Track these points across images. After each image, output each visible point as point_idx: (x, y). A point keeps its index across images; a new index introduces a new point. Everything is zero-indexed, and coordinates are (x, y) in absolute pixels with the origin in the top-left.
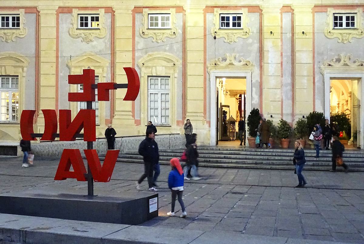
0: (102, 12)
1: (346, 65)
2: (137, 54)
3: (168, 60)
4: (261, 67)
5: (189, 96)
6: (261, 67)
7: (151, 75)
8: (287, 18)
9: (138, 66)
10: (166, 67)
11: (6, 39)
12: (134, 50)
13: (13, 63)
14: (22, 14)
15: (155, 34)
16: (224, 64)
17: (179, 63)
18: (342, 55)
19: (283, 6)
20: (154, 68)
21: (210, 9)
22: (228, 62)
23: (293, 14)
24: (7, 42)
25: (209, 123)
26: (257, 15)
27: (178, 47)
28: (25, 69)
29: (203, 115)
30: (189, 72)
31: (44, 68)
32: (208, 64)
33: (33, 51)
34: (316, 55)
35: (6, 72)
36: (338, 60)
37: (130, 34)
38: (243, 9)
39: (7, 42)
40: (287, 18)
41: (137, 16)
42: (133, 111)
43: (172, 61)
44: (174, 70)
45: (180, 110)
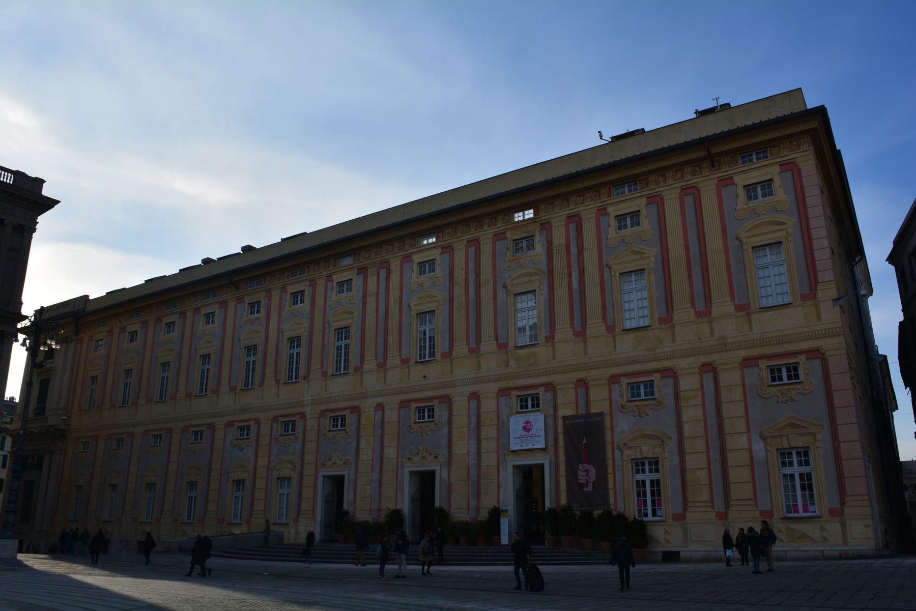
1: (424, 458)
6: (357, 464)
8: (379, 415)
12: (269, 456)
16: (328, 464)
21: (323, 413)
22: (333, 461)
23: (383, 411)
25: (315, 520)
36: (418, 454)
40: (379, 415)
41: (275, 425)
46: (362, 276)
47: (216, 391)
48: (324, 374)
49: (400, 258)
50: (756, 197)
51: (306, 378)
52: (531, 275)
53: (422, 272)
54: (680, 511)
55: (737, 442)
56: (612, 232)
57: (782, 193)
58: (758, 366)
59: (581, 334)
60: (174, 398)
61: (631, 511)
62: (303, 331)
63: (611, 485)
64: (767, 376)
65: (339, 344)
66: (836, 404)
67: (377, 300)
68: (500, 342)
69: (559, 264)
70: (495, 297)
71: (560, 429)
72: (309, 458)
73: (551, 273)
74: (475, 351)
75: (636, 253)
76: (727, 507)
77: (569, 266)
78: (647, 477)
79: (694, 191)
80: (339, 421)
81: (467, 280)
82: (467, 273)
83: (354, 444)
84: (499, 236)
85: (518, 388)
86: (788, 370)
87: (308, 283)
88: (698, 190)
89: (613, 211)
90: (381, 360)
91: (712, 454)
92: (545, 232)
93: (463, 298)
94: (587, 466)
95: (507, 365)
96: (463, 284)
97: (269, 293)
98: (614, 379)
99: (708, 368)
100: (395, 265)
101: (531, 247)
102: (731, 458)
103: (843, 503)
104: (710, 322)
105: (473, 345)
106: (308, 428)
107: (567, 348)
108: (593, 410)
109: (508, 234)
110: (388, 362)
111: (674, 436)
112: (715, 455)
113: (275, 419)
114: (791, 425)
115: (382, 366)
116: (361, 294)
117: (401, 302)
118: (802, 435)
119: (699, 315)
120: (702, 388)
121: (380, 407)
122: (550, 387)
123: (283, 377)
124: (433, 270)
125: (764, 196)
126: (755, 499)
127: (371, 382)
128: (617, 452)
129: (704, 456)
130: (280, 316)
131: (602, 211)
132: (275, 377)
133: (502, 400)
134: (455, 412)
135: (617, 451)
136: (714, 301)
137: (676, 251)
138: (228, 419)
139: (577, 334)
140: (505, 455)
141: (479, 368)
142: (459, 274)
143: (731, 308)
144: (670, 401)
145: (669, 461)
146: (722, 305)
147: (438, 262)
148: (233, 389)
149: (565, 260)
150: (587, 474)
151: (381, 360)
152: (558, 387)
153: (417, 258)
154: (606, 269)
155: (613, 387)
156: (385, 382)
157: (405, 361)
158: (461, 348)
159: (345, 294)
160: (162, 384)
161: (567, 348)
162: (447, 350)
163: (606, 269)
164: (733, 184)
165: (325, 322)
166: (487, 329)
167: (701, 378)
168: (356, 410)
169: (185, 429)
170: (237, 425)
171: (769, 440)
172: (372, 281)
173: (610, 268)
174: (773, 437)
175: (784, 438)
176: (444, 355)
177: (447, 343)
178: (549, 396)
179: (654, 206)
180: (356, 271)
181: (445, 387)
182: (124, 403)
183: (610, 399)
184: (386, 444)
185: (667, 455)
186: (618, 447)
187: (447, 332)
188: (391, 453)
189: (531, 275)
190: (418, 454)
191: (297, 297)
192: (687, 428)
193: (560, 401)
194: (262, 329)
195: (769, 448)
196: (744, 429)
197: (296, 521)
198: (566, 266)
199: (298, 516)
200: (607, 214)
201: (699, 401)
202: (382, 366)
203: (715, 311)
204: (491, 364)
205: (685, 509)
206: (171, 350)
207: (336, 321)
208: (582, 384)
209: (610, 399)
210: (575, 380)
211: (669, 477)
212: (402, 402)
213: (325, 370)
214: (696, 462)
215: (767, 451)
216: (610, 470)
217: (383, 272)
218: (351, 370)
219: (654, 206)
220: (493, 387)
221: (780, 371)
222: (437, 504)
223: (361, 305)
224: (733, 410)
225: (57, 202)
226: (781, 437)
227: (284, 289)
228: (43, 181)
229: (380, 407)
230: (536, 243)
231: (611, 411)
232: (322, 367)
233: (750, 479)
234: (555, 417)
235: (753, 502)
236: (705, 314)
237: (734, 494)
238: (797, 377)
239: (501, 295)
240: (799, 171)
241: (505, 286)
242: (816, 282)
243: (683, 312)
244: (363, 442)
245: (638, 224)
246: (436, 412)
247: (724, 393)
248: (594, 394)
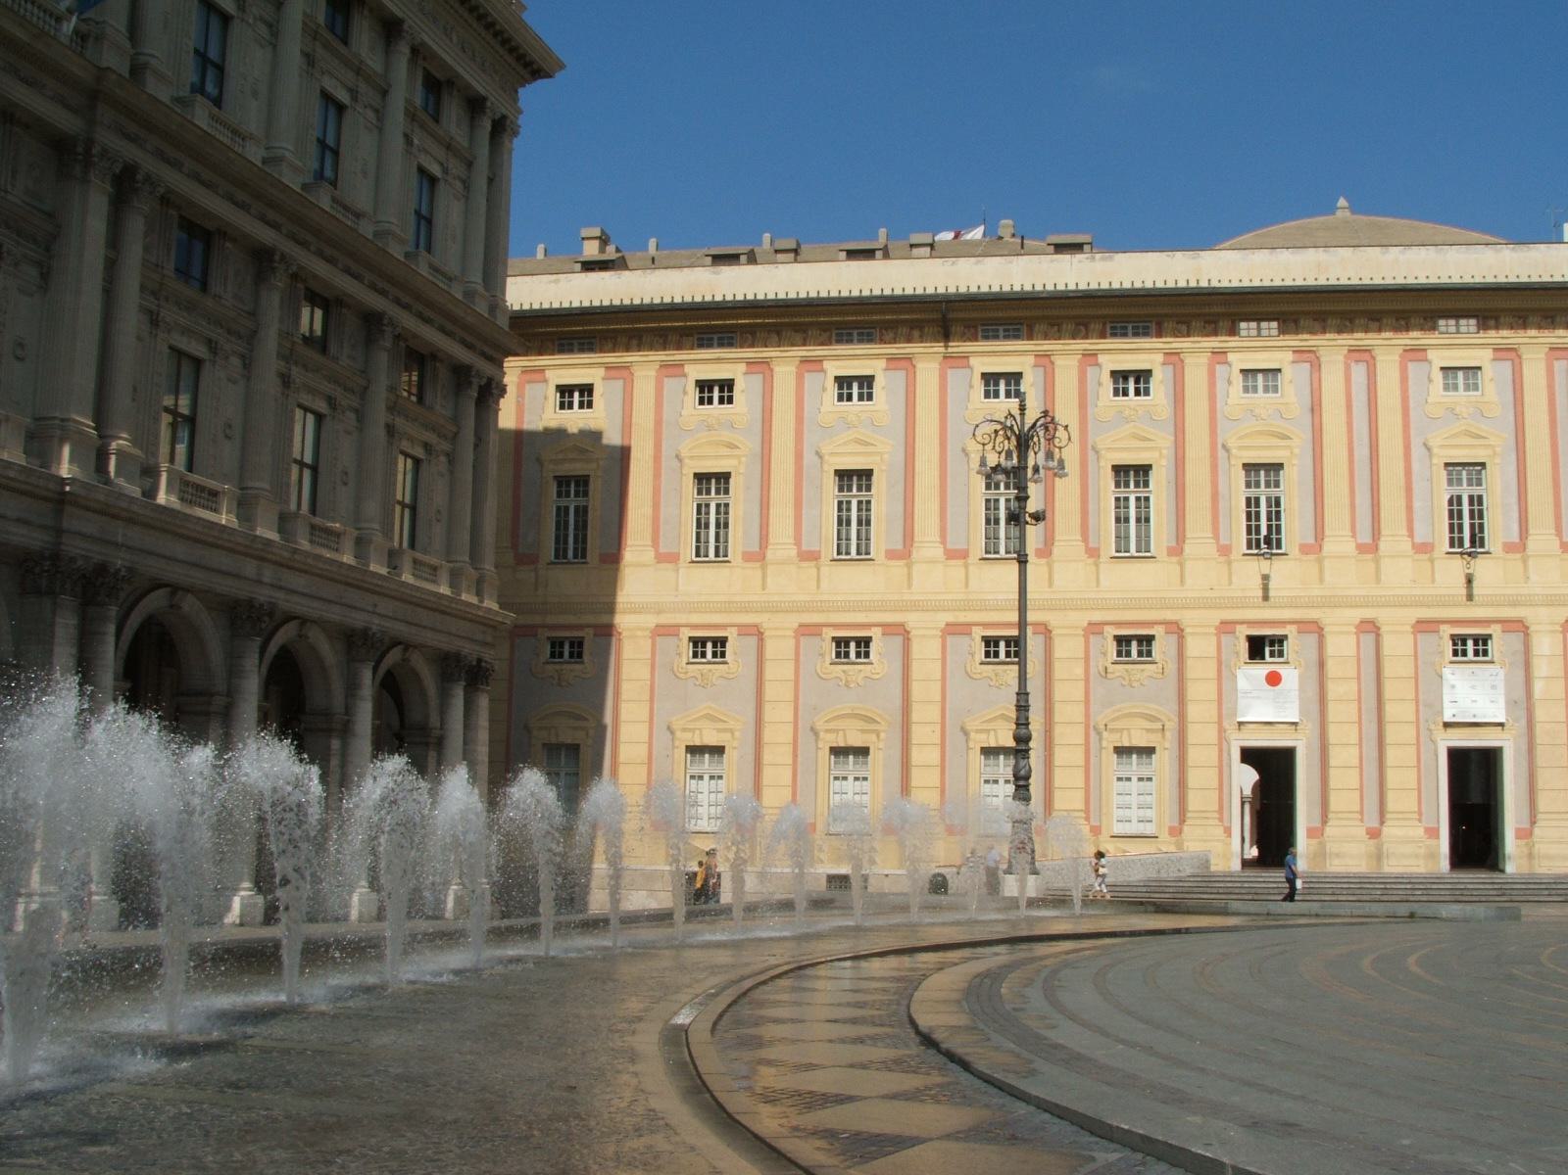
3: (1152, 718)
7: (1120, 745)
9: (1095, 728)
10: (1148, 730)
11: (847, 681)
13: (861, 725)
14: (875, 633)
15: (1127, 671)
17: (1172, 725)
19: (1362, 622)
20: (1125, 732)
23: (1378, 635)
24: (847, 686)
26: (1313, 639)
27: (1171, 691)
28: (882, 735)
29: (1216, 815)
30: (1191, 738)
31: (918, 734)
32: (1226, 724)
33: (898, 702)
34: (1421, 708)
35: (845, 741)
37: (1079, 671)
38: (1289, 627)
39: (847, 686)
40: (1368, 639)
42: (1087, 811)
43: (1159, 720)
44: (1164, 737)
45: (1176, 808)
47: (904, 552)
48: (1225, 551)
49: (1400, 350)
62: (1156, 453)
65: (1253, 492)
97: (1044, 360)
110: (1382, 545)
113: (1094, 629)
115: (1370, 548)
123: (1110, 547)
132: (1085, 537)
138: (950, 617)
153: (1439, 358)
156: (1378, 580)
162: (1517, 540)
168: (1316, 629)
170: (978, 633)
176: (1509, 548)
177: (1515, 527)
181: (1514, 604)
182: (560, 553)
187: (1515, 508)
199: (1182, 820)
206: (732, 446)
207: (1240, 448)
212: (1419, 622)
213: (1223, 542)
217: (1359, 372)
227: (1090, 357)
232: (1216, 536)
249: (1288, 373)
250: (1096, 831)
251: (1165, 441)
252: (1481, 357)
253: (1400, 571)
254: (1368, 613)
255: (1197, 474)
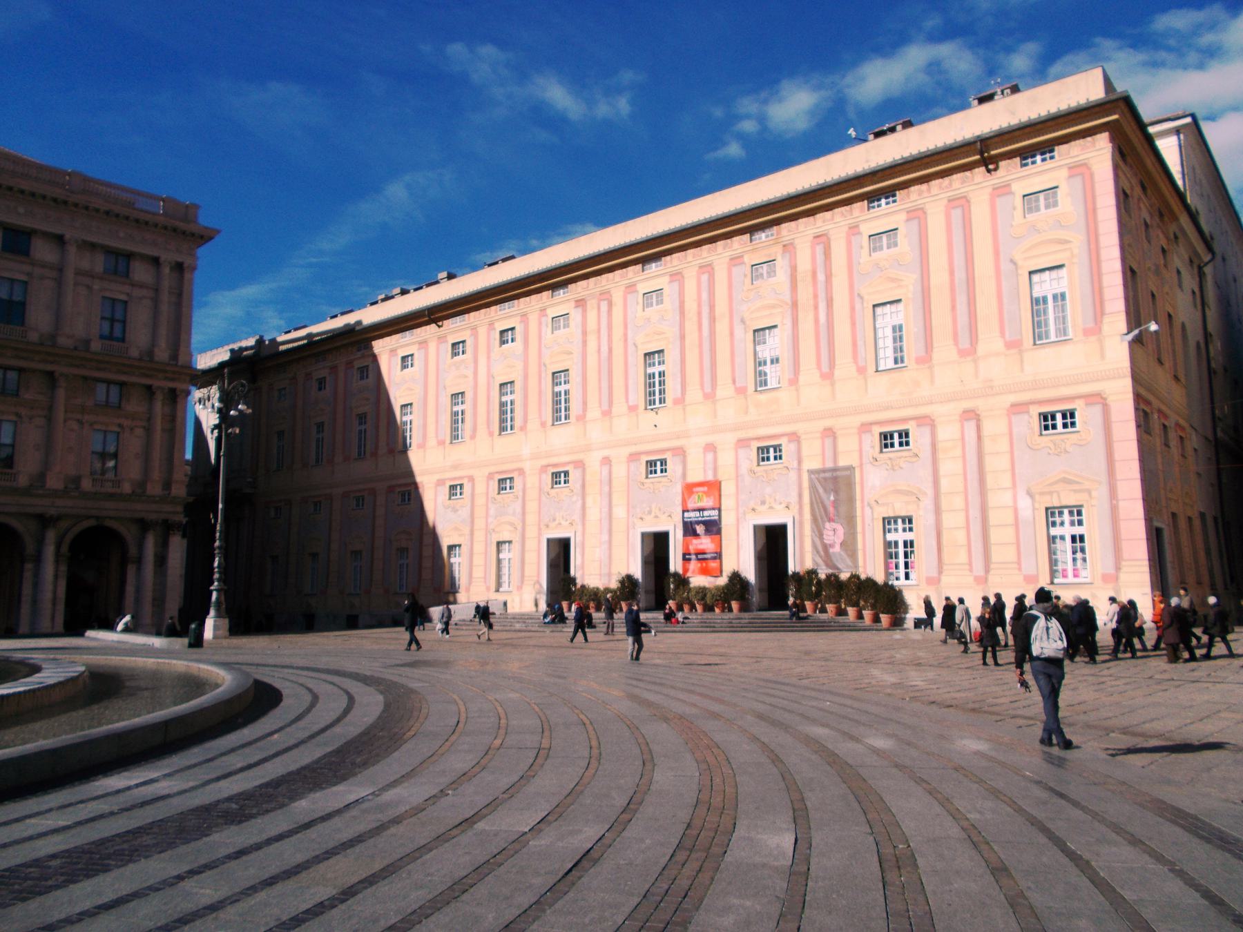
0: (465, 482)
1: (656, 517)
2: (490, 520)
3: (512, 524)
4: (584, 525)
5: (527, 561)
6: (584, 525)
8: (605, 470)
16: (553, 525)
17: (519, 527)
18: (653, 506)
27: (519, 510)
40: (605, 470)
41: (491, 483)
46: (580, 310)
48: (543, 424)
50: (1038, 209)
51: (523, 428)
52: (774, 307)
53: (647, 305)
54: (934, 574)
55: (1000, 499)
56: (863, 256)
57: (1068, 203)
58: (1028, 412)
59: (828, 376)
60: (375, 454)
61: (880, 578)
62: (516, 375)
63: (860, 546)
64: (1036, 423)
66: (1117, 456)
67: (599, 338)
68: (738, 385)
69: (805, 293)
70: (732, 334)
71: (806, 484)
72: (531, 518)
73: (795, 305)
74: (710, 397)
75: (893, 280)
76: (987, 570)
77: (816, 296)
78: (899, 536)
79: (962, 202)
80: (559, 477)
81: (699, 314)
82: (699, 306)
83: (580, 503)
84: (736, 260)
85: (758, 439)
86: (1064, 417)
87: (518, 318)
88: (968, 201)
89: (867, 229)
90: (605, 407)
91: (971, 512)
92: (788, 255)
93: (696, 334)
94: (834, 525)
95: (746, 412)
96: (695, 319)
98: (865, 428)
99: (972, 415)
100: (617, 296)
101: (772, 273)
102: (994, 518)
103: (1118, 568)
104: (975, 361)
105: (708, 389)
106: (529, 485)
107: (812, 392)
108: (842, 463)
109: (746, 259)
111: (930, 492)
112: (975, 513)
114: (1066, 481)
115: (607, 413)
116: (580, 331)
117: (626, 340)
118: (1075, 491)
119: (963, 353)
120: (963, 439)
121: (607, 461)
122: (794, 437)
124: (660, 302)
125: (1047, 207)
126: (1019, 563)
127: (596, 432)
128: (867, 510)
129: (963, 514)
130: (489, 358)
131: (854, 229)
132: (488, 427)
133: (742, 452)
134: (690, 465)
135: (867, 510)
136: (980, 336)
137: (939, 277)
138: (437, 477)
139: (824, 376)
140: (744, 514)
141: (715, 417)
142: (691, 305)
143: (999, 345)
144: (926, 453)
145: (924, 521)
146: (990, 341)
147: (666, 292)
148: (441, 443)
149: (811, 289)
150: (835, 534)
151: (605, 407)
152: (803, 437)
154: (857, 300)
155: (864, 436)
157: (633, 409)
158: (694, 394)
159: (562, 331)
160: (360, 439)
161: (812, 392)
163: (857, 300)
164: (1011, 193)
165: (541, 365)
166: (723, 371)
167: (962, 427)
168: (580, 464)
169: (391, 489)
171: (1037, 497)
172: (592, 315)
173: (862, 298)
174: (1042, 494)
175: (1055, 495)
177: (679, 387)
178: (793, 446)
179: (915, 222)
180: (573, 304)
181: (678, 438)
183: (861, 451)
184: (614, 502)
185: (921, 513)
186: (869, 505)
188: (620, 512)
189: (774, 307)
190: (650, 512)
191: (505, 335)
192: (944, 483)
193: (805, 452)
194: (470, 373)
195: (1037, 506)
196: (1008, 484)
197: (520, 588)
198: (811, 296)
199: (522, 582)
200: (859, 233)
201: (958, 452)
202: (607, 413)
203: (981, 349)
204: (729, 411)
205: (940, 572)
208: (830, 433)
209: (861, 451)
210: (821, 429)
211: (922, 535)
214: (953, 520)
215: (1034, 509)
216: (859, 529)
218: (572, 419)
219: (915, 222)
220: (731, 438)
221: (1053, 418)
222: (672, 569)
223: (580, 345)
224: (997, 464)
225: (218, 232)
226: (1051, 493)
228: (196, 207)
229: (607, 461)
230: (778, 269)
231: (861, 465)
233: (1014, 541)
234: (799, 470)
235: (1016, 566)
236: (969, 352)
237: (996, 556)
238: (1073, 424)
239: (739, 331)
240: (1092, 175)
241: (743, 321)
242: (1103, 314)
243: (944, 350)
244: (589, 500)
245: (896, 245)
246: (669, 466)
247: (988, 446)
248: (842, 446)
249: (572, 316)
250: (488, 589)
251: (519, 365)
252: (662, 282)
253: (622, 425)
254: (606, 453)
255: (533, 382)
